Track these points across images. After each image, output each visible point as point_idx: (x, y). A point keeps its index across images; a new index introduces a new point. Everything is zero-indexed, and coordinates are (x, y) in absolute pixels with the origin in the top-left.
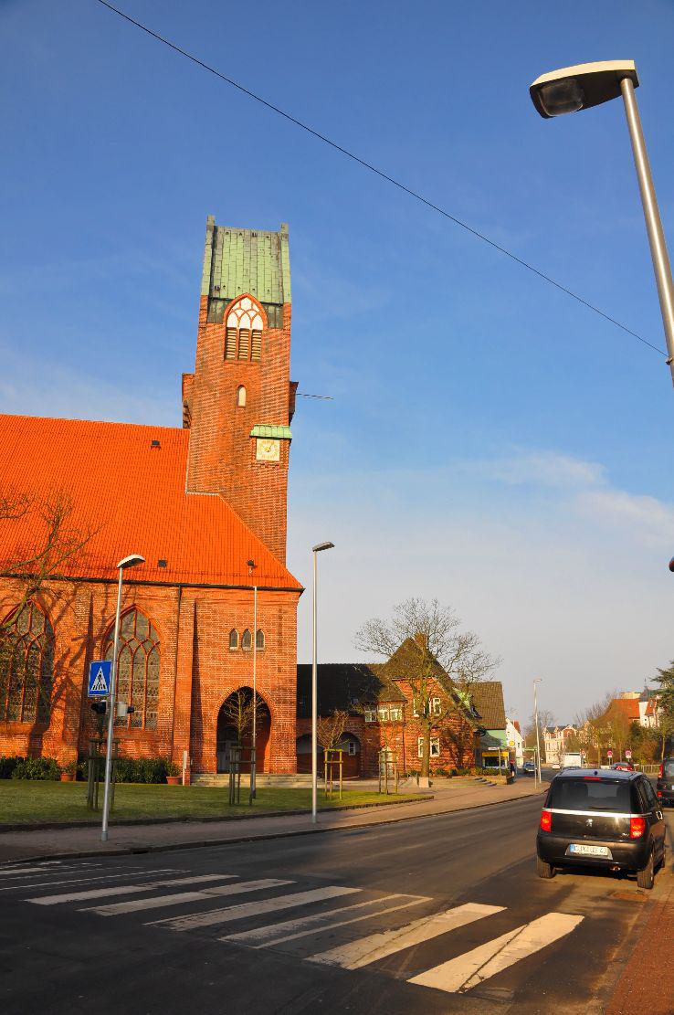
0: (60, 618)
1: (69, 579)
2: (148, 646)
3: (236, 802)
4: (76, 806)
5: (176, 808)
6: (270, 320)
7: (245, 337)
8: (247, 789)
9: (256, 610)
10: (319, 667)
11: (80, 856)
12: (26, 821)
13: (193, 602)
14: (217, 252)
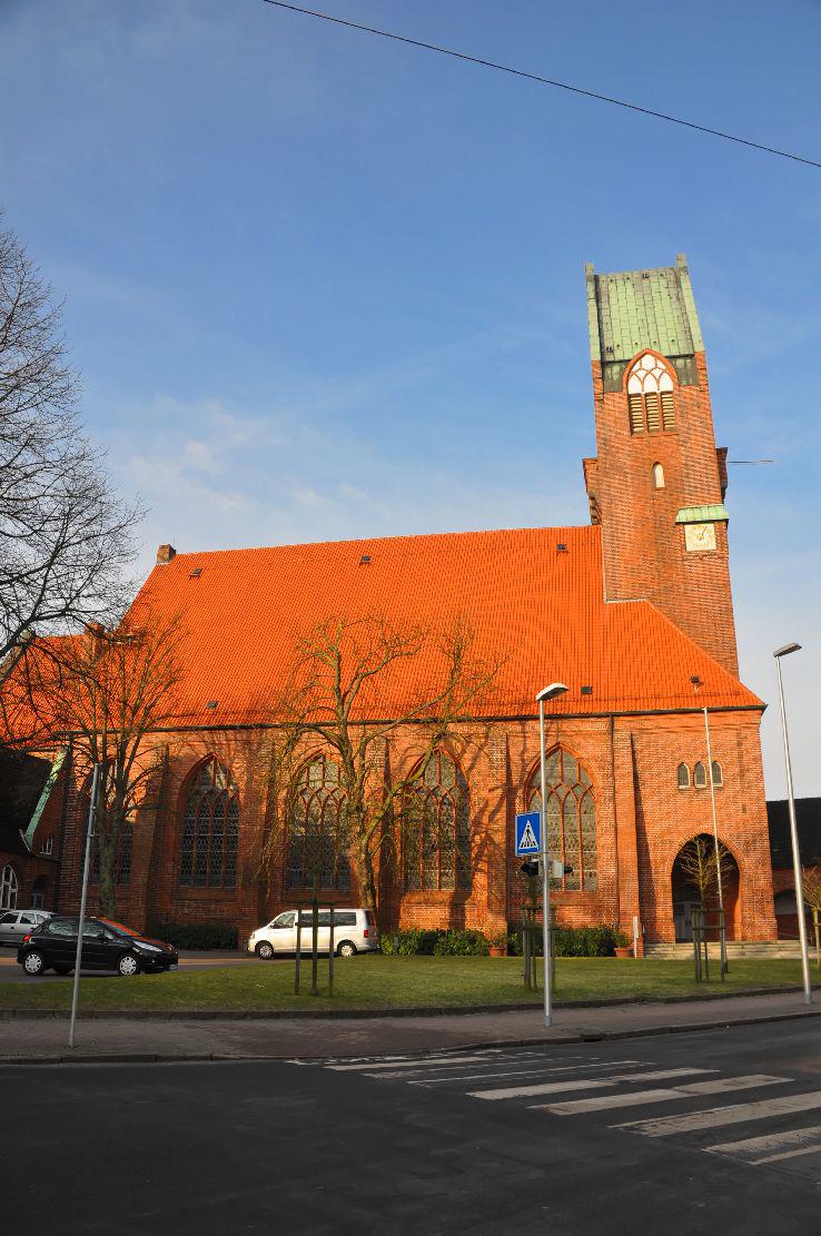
0: (471, 768)
1: (478, 720)
2: (579, 791)
3: (704, 977)
4: (512, 986)
5: (631, 986)
6: (680, 377)
8: (716, 961)
9: (708, 737)
10: (797, 802)
11: (522, 1044)
12: (456, 1004)
14: (604, 305)
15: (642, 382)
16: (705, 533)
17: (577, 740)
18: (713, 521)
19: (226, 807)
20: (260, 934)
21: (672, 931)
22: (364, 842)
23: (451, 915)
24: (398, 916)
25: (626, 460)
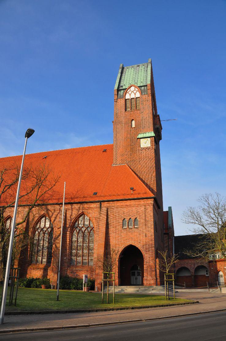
0: (54, 220)
1: (57, 204)
2: (89, 229)
7: (134, 103)
13: (106, 209)
14: (123, 75)
15: (130, 95)
18: (150, 137)
21: (117, 281)
22: (3, 244)
23: (44, 272)
24: (26, 273)
25: (123, 119)
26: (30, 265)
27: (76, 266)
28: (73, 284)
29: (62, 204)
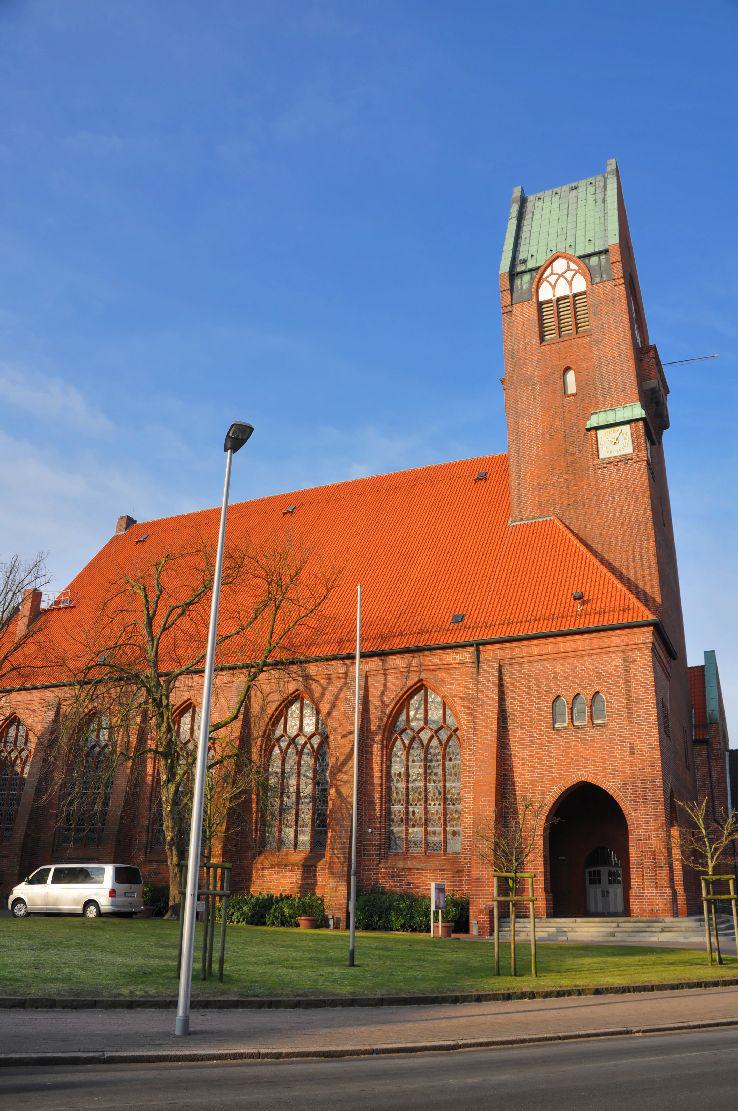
1: (335, 658)
2: (444, 735)
6: (590, 275)
13: (496, 665)
14: (525, 222)
15: (554, 287)
16: (621, 438)
17: (441, 675)
19: (97, 759)
20: (22, 890)
21: (542, 904)
23: (304, 878)
24: (249, 879)
25: (532, 369)
26: (260, 853)
27: (406, 855)
28: (399, 912)
29: (354, 658)
